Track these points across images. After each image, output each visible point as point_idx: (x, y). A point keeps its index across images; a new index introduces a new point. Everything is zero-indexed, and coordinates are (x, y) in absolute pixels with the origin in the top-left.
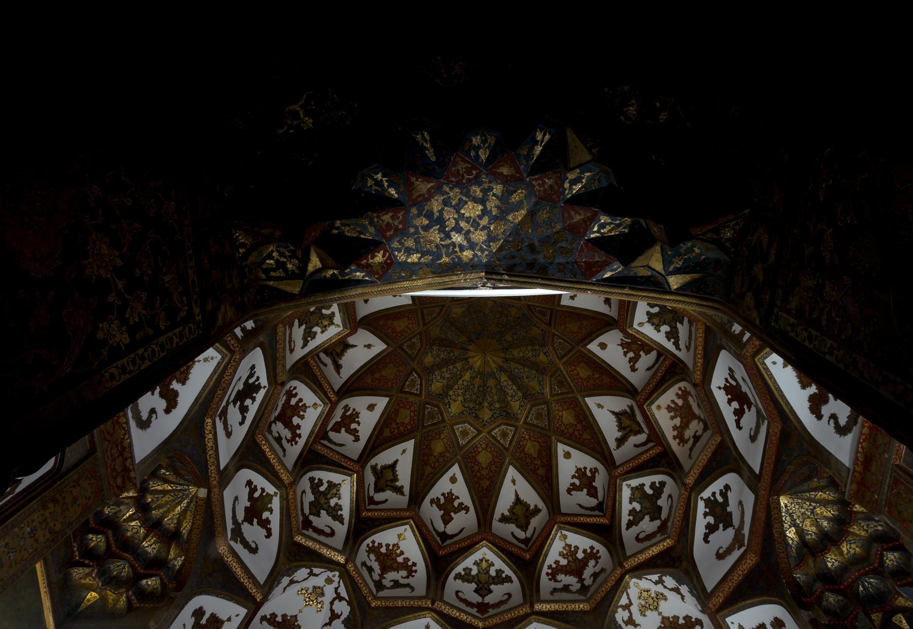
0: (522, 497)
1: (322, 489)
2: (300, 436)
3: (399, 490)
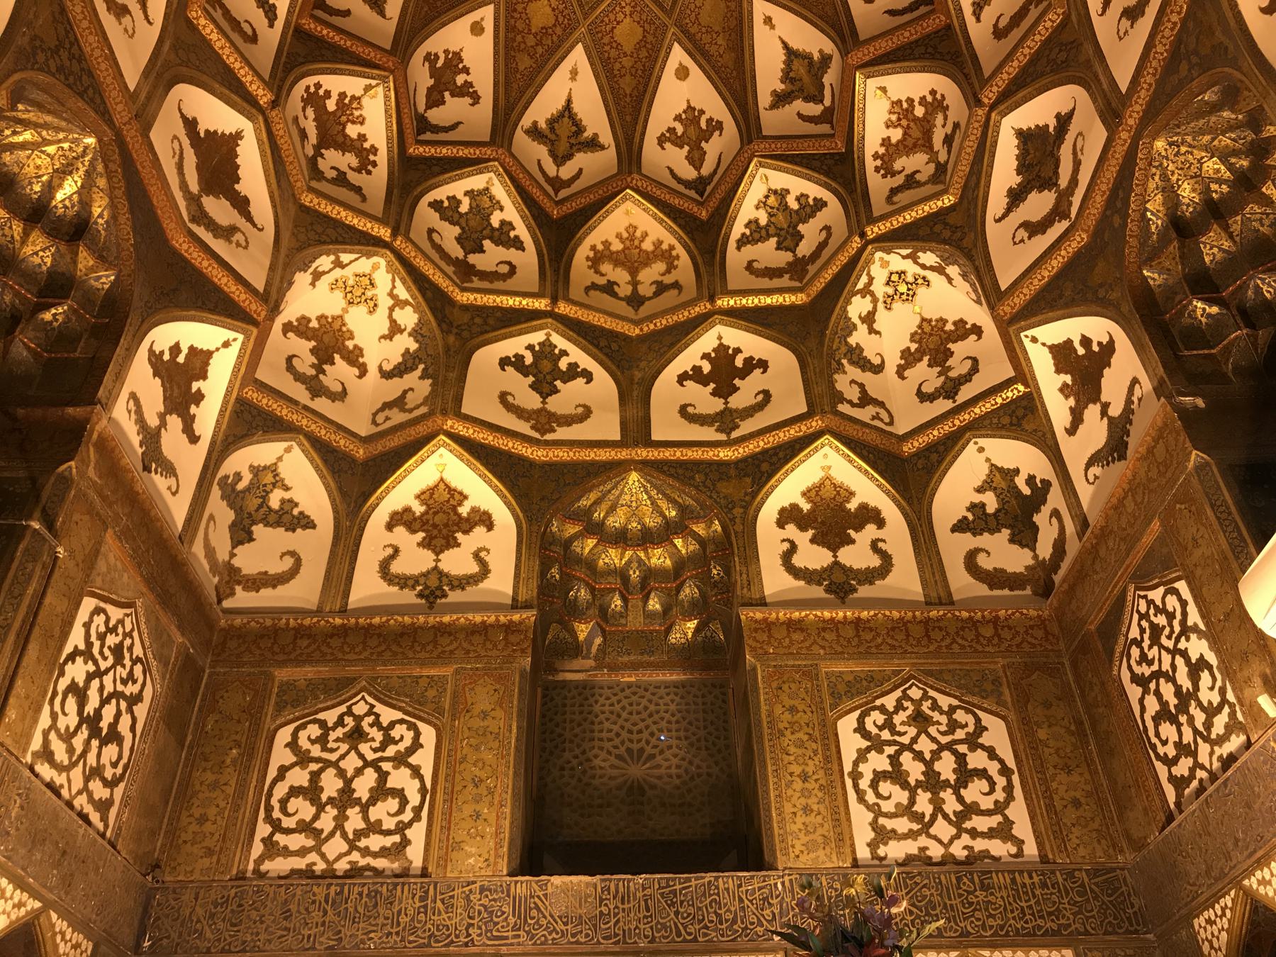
0: (795, 45)
1: (464, 208)
2: (374, 150)
3: (593, 144)
